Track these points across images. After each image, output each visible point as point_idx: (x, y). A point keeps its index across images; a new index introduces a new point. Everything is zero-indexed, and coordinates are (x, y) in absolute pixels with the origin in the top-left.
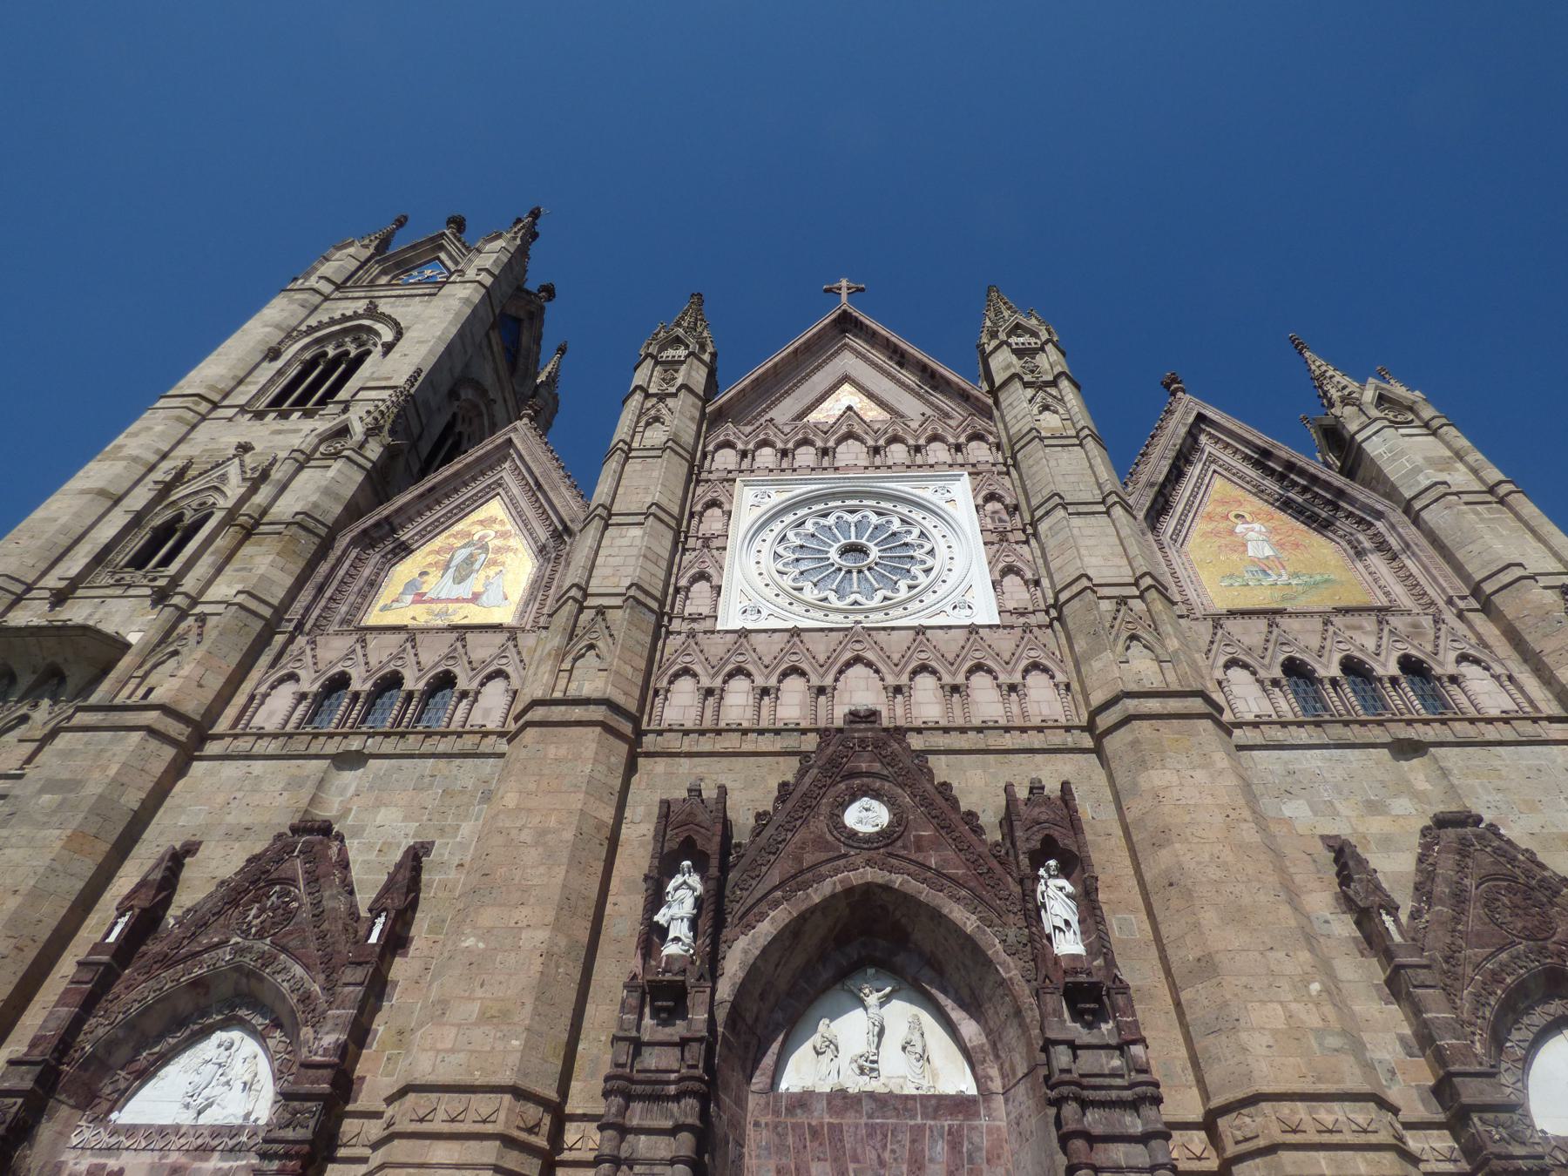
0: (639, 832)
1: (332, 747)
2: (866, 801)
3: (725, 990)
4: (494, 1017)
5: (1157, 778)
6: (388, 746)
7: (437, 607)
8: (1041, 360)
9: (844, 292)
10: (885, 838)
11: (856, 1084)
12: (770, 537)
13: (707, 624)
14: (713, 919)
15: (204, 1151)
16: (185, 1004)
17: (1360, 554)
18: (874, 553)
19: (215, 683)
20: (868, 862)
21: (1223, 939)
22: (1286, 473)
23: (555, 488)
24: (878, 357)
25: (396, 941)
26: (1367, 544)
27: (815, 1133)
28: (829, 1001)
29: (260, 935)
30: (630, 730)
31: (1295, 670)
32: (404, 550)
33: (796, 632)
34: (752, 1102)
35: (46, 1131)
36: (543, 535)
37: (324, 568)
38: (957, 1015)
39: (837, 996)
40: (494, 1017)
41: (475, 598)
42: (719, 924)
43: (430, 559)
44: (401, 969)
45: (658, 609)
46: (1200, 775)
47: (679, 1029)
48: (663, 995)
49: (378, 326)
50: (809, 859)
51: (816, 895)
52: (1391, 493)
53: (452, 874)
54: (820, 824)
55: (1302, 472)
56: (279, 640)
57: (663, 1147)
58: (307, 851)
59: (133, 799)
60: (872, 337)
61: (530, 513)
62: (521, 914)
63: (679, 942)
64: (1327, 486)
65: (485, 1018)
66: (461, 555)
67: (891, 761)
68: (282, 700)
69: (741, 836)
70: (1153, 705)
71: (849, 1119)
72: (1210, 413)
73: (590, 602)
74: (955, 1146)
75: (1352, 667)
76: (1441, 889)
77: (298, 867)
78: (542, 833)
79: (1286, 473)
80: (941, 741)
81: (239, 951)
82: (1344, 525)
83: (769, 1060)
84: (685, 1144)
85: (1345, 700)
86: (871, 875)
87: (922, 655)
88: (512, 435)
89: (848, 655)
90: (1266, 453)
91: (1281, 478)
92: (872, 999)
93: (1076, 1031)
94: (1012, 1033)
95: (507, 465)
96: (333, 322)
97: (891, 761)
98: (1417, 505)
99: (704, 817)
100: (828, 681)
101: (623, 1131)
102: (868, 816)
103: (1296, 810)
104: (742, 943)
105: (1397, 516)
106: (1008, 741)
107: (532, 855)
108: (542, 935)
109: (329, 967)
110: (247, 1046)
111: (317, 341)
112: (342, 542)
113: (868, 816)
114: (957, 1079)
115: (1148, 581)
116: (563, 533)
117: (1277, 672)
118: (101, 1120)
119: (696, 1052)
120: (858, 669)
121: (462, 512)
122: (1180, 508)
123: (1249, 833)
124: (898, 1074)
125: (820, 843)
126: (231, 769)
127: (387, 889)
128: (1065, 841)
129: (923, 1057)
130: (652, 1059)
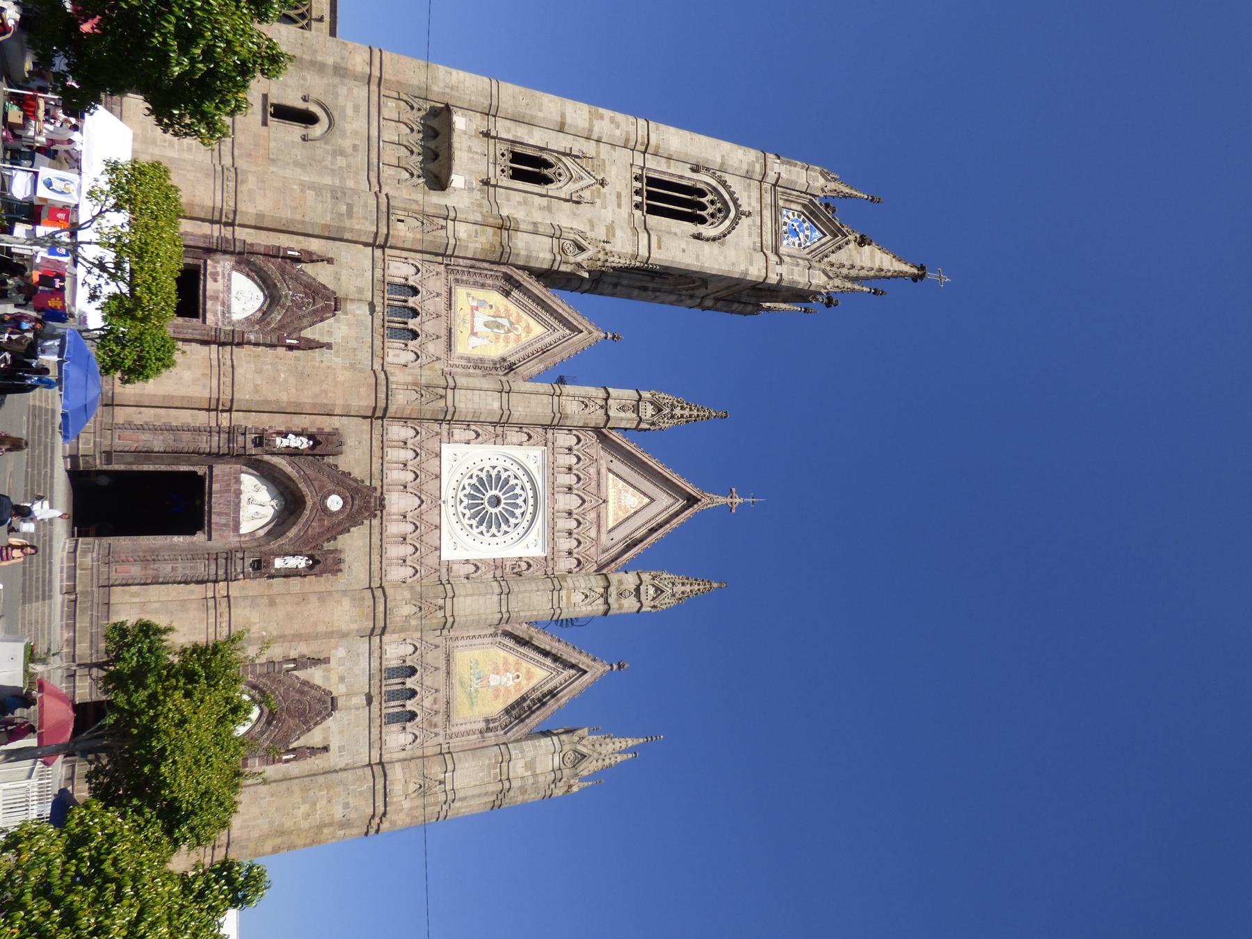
0: (327, 424)
2: (341, 502)
3: (267, 458)
4: (256, 389)
5: (346, 603)
6: (378, 322)
7: (469, 318)
8: (633, 600)
9: (729, 500)
10: (325, 509)
11: (244, 498)
12: (508, 465)
13: (445, 438)
14: (293, 453)
15: (223, 304)
16: (269, 282)
17: (487, 721)
18: (496, 510)
19: (406, 246)
20: (314, 504)
21: (281, 611)
22: (541, 701)
23: (541, 361)
24: (660, 519)
25: (290, 348)
26: (491, 725)
27: (228, 485)
28: (272, 488)
29: (292, 301)
30: (378, 415)
31: (412, 671)
32: (507, 294)
33: (438, 477)
34: (238, 466)
35: (227, 256)
36: (512, 359)
37: (486, 265)
38: (266, 529)
39: (276, 492)
40: (256, 389)
41: (474, 334)
42: (291, 455)
43: (502, 309)
44: (281, 351)
45: (447, 418)
46: (347, 618)
47: (249, 445)
48: (261, 440)
49: (727, 223)
50: (316, 484)
51: (302, 486)
53: (318, 359)
54: (331, 486)
55: (538, 708)
56: (440, 259)
57: (215, 444)
58: (328, 306)
59: (347, 236)
60: (676, 514)
61: (529, 350)
62: (293, 391)
63: (280, 442)
65: (256, 386)
66: (505, 322)
67: (359, 512)
68: (408, 270)
69: (330, 460)
70: (381, 608)
71: (232, 495)
72: (586, 677)
73: (450, 392)
74: (224, 525)
75: (413, 693)
76: (306, 689)
77: (320, 304)
78: (326, 392)
79: (541, 701)
80: (376, 531)
81: (286, 296)
83: (251, 471)
84: (215, 450)
85: (394, 684)
86: (309, 504)
87: (424, 529)
88: (585, 332)
89: (423, 497)
90: (555, 695)
91: (539, 700)
92: (273, 503)
93: (248, 561)
94: (255, 544)
95: (568, 331)
96: (731, 194)
97: (359, 512)
99: (330, 448)
100: (409, 489)
101: (219, 433)
102: (335, 503)
103: (341, 652)
104: (284, 462)
106: (376, 558)
107: (316, 390)
108: (285, 398)
109: (281, 327)
110: (258, 305)
111: (715, 189)
112: (504, 269)
113: (335, 503)
114: (245, 528)
116: (511, 368)
117: (408, 663)
118: (233, 268)
119: (242, 452)
120: (418, 502)
121: (535, 316)
122: (521, 649)
123: (321, 628)
124: (247, 511)
125: (322, 487)
126: (367, 264)
127: (308, 340)
128: (318, 568)
129: (253, 518)
130: (241, 438)
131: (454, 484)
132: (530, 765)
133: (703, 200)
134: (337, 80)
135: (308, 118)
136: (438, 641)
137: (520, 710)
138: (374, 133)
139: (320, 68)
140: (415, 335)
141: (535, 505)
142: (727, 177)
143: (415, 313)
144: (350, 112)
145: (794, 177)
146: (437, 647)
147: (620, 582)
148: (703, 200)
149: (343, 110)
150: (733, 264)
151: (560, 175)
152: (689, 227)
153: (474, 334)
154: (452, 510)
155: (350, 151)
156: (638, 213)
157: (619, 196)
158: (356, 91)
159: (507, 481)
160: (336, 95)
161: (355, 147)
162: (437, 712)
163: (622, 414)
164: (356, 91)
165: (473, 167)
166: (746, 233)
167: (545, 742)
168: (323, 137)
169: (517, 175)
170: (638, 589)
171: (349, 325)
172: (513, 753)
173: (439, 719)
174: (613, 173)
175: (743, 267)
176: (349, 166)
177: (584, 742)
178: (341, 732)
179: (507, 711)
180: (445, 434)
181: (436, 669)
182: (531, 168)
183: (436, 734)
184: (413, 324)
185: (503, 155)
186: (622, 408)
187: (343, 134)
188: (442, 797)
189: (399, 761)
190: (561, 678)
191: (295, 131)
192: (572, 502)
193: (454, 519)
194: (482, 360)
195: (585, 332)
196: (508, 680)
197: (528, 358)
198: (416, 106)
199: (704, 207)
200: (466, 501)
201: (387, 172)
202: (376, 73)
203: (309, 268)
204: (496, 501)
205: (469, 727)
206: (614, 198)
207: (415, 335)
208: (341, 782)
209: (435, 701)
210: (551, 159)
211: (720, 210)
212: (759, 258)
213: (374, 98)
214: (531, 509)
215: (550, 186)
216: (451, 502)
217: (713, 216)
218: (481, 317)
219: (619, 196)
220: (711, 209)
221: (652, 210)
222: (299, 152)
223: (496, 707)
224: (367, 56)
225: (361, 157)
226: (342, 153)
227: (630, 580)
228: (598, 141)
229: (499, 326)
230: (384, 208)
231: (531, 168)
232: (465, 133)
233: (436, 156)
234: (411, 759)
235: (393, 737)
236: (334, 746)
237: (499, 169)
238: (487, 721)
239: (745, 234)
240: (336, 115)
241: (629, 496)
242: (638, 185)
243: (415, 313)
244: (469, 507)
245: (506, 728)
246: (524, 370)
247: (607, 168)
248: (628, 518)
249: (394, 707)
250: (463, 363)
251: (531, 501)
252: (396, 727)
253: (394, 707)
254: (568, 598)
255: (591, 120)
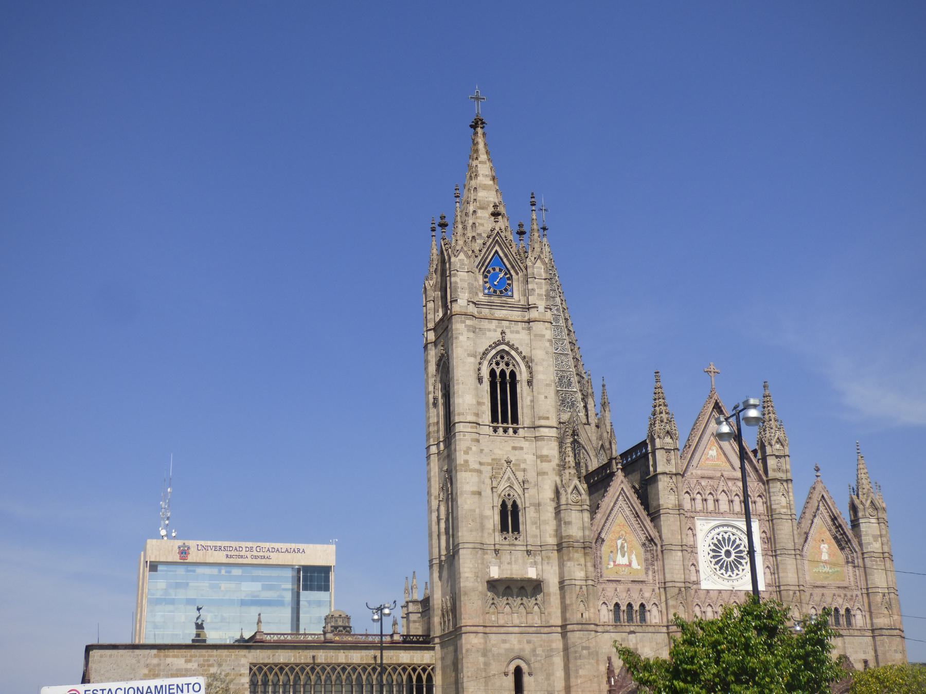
1: (628, 629)
17: (848, 562)
32: (603, 540)
33: (720, 591)
49: (513, 353)
52: (861, 545)
55: (843, 529)
61: (636, 526)
64: (847, 537)
66: (619, 542)
79: (839, 527)
82: (847, 551)
90: (836, 518)
91: (837, 527)
98: (865, 556)
105: (860, 555)
115: (802, 588)
131: (721, 580)
132: (875, 538)
133: (498, 374)
134: (490, 654)
135: (518, 672)
136: (808, 594)
137: (842, 541)
138: (516, 630)
139: (486, 664)
140: (642, 605)
141: (728, 526)
142: (482, 350)
143: (630, 605)
144: (507, 646)
145: (466, 285)
146: (811, 594)
147: (774, 470)
148: (498, 374)
149: (507, 650)
150: (547, 353)
151: (509, 495)
152: (522, 389)
153: (630, 565)
154: (735, 583)
155: (531, 646)
156: (521, 431)
157: (514, 448)
158: (493, 642)
159: (715, 545)
160: (499, 655)
161: (529, 642)
162: (845, 595)
163: (673, 462)
164: (493, 642)
165: (520, 561)
166: (517, 336)
167: (863, 527)
168: (528, 664)
169: (516, 528)
170: (777, 457)
171: (644, 646)
172: (870, 550)
173: (849, 594)
174: (500, 452)
175: (548, 344)
176: (541, 646)
177: (864, 501)
178: (856, 652)
179: (842, 549)
180: (695, 586)
181: (823, 595)
182: (510, 517)
183: (857, 596)
184: (636, 607)
185: (505, 538)
186: (668, 461)
187: (522, 650)
188: (892, 596)
189: (871, 619)
190: (824, 512)
191: (526, 679)
192: (723, 498)
193: (740, 581)
194: (646, 560)
195: (622, 486)
196: (824, 547)
197: (643, 527)
198: (491, 602)
199: (503, 372)
200: (729, 573)
201: (537, 621)
202: (481, 629)
203: (617, 672)
204: (728, 553)
205: (851, 574)
206: (517, 452)
207: (642, 606)
208: (884, 654)
209: (840, 596)
210: (500, 502)
211: (502, 358)
212: (538, 327)
213: (494, 629)
214: (730, 529)
215: (519, 502)
216: (731, 582)
217: (507, 364)
218: (622, 560)
219: (514, 448)
220: (502, 366)
221: (515, 420)
222: (541, 677)
223: (840, 556)
224: (472, 635)
225: (534, 638)
226: (534, 650)
227: (771, 462)
228: (481, 464)
229: (622, 547)
230: (580, 626)
231: (510, 517)
232: (500, 567)
233: (522, 588)
234: (870, 612)
235: (858, 622)
236: (863, 657)
237: (517, 542)
238: (848, 562)
239: (518, 337)
240: (512, 655)
241: (711, 452)
242: (501, 430)
243: (630, 605)
244: (732, 571)
245: (853, 550)
246: (654, 533)
247: (497, 457)
248: (725, 454)
249: (843, 621)
250: (650, 573)
251: (725, 529)
252: (853, 621)
253: (843, 621)
254: (783, 507)
255: (471, 471)
